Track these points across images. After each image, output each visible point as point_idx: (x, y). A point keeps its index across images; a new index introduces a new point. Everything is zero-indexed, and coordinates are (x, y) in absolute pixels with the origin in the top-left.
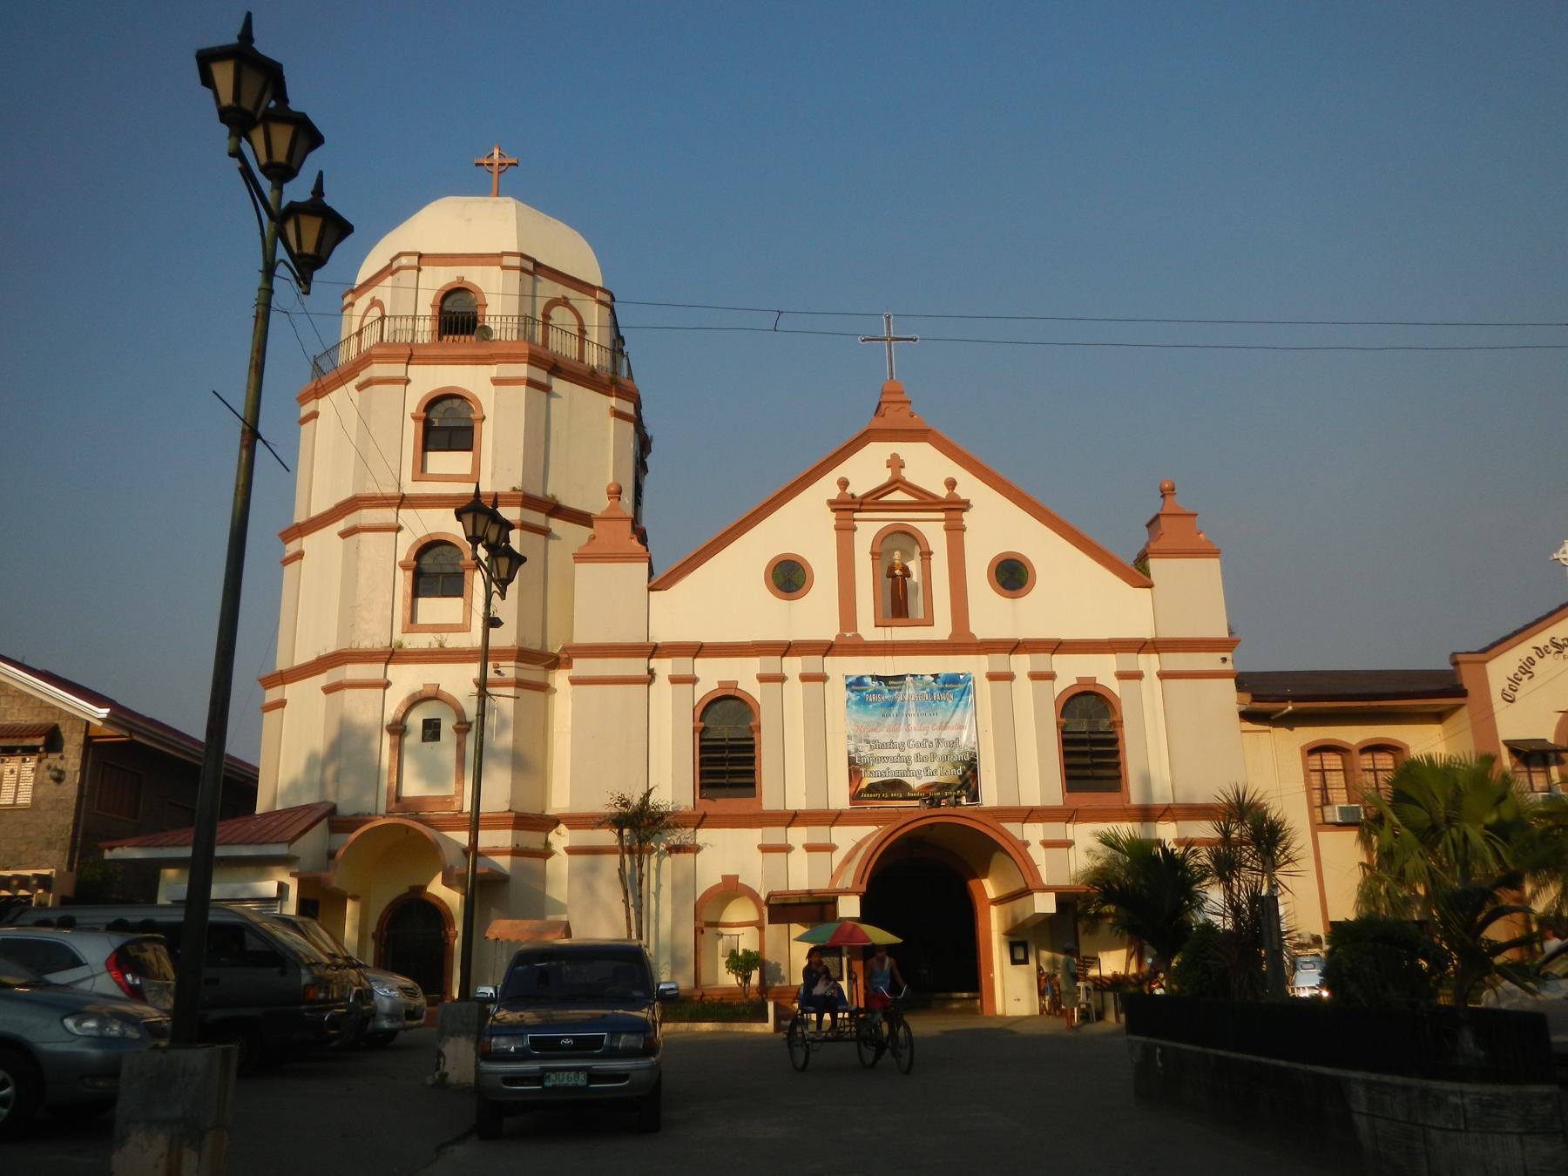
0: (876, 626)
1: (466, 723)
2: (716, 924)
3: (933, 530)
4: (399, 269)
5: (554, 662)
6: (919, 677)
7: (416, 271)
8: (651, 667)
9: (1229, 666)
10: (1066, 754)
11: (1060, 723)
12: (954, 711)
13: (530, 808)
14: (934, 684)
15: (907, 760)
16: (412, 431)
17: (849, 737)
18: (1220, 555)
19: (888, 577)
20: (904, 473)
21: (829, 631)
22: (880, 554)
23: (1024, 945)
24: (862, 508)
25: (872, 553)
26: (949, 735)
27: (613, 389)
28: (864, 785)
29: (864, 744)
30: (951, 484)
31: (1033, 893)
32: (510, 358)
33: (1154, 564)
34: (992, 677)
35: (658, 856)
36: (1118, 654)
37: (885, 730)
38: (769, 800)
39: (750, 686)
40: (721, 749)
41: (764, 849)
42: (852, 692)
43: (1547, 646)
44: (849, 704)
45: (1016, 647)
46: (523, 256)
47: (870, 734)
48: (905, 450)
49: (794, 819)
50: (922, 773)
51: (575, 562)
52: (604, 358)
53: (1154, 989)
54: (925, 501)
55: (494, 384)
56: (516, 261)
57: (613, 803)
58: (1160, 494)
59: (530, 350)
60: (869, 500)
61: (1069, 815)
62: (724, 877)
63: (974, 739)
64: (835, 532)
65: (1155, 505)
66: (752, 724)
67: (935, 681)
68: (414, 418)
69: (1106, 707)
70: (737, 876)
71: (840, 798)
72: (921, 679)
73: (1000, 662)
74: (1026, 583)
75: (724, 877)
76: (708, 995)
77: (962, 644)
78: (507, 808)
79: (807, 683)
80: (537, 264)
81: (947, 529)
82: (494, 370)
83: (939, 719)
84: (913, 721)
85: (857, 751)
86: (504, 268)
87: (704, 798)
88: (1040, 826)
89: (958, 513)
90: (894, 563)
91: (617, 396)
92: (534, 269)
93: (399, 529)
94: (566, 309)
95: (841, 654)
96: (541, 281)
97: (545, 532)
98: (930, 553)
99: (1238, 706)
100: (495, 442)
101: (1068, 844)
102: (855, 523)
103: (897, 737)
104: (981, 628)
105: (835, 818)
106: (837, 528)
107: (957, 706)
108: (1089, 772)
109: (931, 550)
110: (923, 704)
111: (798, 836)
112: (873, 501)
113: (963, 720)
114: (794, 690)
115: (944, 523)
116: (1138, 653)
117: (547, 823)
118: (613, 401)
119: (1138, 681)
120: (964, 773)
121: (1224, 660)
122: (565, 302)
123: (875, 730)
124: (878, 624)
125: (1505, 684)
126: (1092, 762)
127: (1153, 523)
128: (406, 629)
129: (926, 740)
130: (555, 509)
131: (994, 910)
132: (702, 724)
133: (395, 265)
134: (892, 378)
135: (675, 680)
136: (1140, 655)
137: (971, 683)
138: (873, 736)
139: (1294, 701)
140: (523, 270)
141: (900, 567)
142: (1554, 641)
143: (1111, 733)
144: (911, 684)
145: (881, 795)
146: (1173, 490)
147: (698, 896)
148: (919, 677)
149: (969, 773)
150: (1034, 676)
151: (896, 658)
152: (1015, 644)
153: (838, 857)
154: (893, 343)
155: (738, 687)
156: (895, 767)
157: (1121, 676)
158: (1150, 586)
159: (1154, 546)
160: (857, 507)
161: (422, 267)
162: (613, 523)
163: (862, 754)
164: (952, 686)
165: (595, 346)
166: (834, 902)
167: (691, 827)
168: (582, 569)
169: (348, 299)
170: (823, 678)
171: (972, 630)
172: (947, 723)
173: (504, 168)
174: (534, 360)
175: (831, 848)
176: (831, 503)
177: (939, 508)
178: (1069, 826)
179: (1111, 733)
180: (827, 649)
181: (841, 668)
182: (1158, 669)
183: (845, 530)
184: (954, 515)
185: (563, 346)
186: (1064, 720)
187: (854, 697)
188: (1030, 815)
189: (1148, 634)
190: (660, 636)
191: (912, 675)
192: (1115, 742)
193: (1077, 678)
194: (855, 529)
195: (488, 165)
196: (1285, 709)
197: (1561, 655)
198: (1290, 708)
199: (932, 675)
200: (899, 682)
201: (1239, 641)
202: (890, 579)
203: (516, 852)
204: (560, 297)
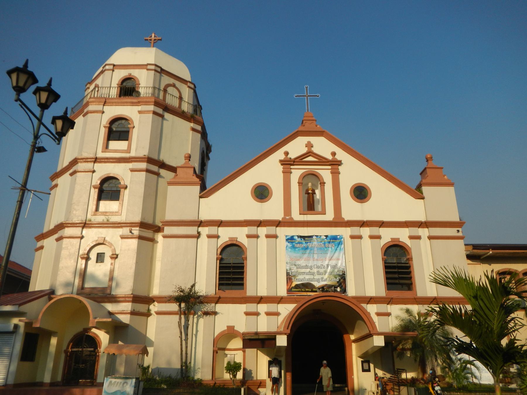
0: (300, 214)
1: (115, 254)
2: (224, 349)
3: (326, 174)
4: (105, 70)
5: (158, 230)
6: (319, 237)
7: (112, 71)
8: (199, 231)
9: (460, 234)
10: (387, 273)
11: (384, 258)
12: (335, 252)
13: (141, 293)
14: (326, 240)
15: (313, 274)
16: (103, 132)
17: (287, 263)
18: (454, 185)
19: (306, 194)
20: (313, 149)
21: (279, 216)
22: (302, 183)
23: (368, 362)
24: (294, 163)
25: (299, 183)
26: (333, 263)
27: (192, 119)
28: (293, 285)
29: (294, 266)
30: (334, 154)
31: (373, 336)
32: (146, 103)
33: (424, 189)
34: (352, 237)
35: (197, 317)
36: (409, 228)
37: (303, 260)
38: (250, 291)
39: (243, 240)
40: (229, 268)
41: (247, 314)
42: (289, 242)
44: (287, 248)
45: (363, 224)
46: (156, 65)
47: (296, 262)
48: (313, 140)
49: (260, 300)
50: (320, 280)
51: (168, 185)
52: (189, 108)
53: (435, 387)
54: (322, 161)
55: (139, 113)
56: (153, 67)
57: (176, 290)
58: (426, 160)
59: (155, 99)
60: (297, 160)
61: (389, 301)
62: (228, 327)
63: (344, 265)
64: (282, 174)
65: (425, 165)
66: (243, 256)
67: (326, 238)
68: (105, 127)
69: (404, 252)
70: (234, 326)
71: (282, 291)
72: (320, 237)
73: (356, 230)
74: (367, 196)
75: (228, 327)
76: (218, 383)
77: (338, 222)
78: (131, 293)
79: (268, 239)
80: (162, 69)
81: (332, 173)
82: (139, 108)
83: (329, 255)
84: (316, 256)
85: (290, 269)
86: (148, 70)
87: (220, 290)
88: (375, 305)
89: (338, 166)
90: (308, 188)
91: (194, 123)
92: (161, 71)
93: (94, 172)
95: (284, 226)
96: (164, 76)
97: (158, 174)
98: (324, 183)
99: (465, 252)
100: (138, 137)
101: (389, 314)
102: (291, 170)
103: (309, 263)
104: (347, 215)
105: (280, 300)
106: (283, 172)
107: (336, 250)
108: (397, 281)
109: (325, 181)
110: (321, 249)
111: (263, 308)
112: (300, 160)
113: (339, 256)
114: (263, 242)
115: (330, 170)
116: (419, 228)
117: (149, 300)
118: (192, 125)
119: (419, 240)
120: (340, 280)
121: (458, 231)
122: (174, 86)
123: (299, 260)
124: (301, 213)
126: (399, 276)
127: (423, 173)
128: (93, 214)
129: (322, 265)
130: (163, 165)
131: (354, 345)
132: (221, 256)
133: (104, 70)
134: (308, 111)
135: (209, 236)
136: (419, 229)
137: (342, 240)
138: (298, 263)
139: (492, 249)
140: (155, 71)
141: (311, 189)
143: (407, 263)
144: (315, 240)
145: (301, 290)
146: (432, 158)
147: (216, 335)
148: (319, 237)
149: (342, 280)
150: (371, 237)
151: (308, 228)
152: (363, 223)
153: (281, 318)
154: (309, 97)
155: (238, 240)
156: (307, 277)
157: (411, 237)
158: (423, 198)
159: (424, 181)
160: (292, 163)
161: (114, 70)
162: (185, 169)
163: (293, 271)
164: (334, 241)
165: (187, 103)
166: (275, 339)
167: (213, 303)
168: (171, 188)
169: (88, 86)
170: (275, 237)
171: (343, 216)
172: (332, 257)
173: (156, 41)
174: (157, 104)
175: (277, 314)
176: (281, 161)
177: (328, 164)
178: (389, 306)
179: (407, 263)
180: (278, 224)
181: (284, 232)
182: (428, 235)
183: (287, 173)
184: (335, 167)
185: (172, 101)
186: (385, 257)
187: (289, 245)
188: (371, 300)
189: (423, 219)
190: (204, 216)
191: (317, 236)
192: (409, 267)
193: (391, 238)
194: (291, 173)
195: (150, 40)
196: (489, 253)
198: (491, 252)
199: (325, 236)
200: (310, 239)
201: (465, 223)
202: (307, 195)
203: (133, 313)
204: (172, 83)
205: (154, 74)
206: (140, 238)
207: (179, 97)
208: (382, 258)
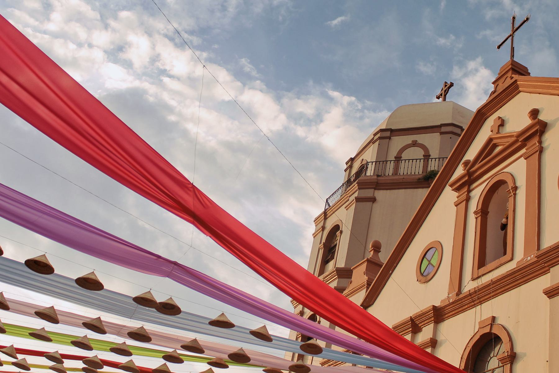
30: (534, 113)
46: (382, 130)
56: (378, 135)
122: (415, 144)
160: (466, 178)
205: (379, 144)
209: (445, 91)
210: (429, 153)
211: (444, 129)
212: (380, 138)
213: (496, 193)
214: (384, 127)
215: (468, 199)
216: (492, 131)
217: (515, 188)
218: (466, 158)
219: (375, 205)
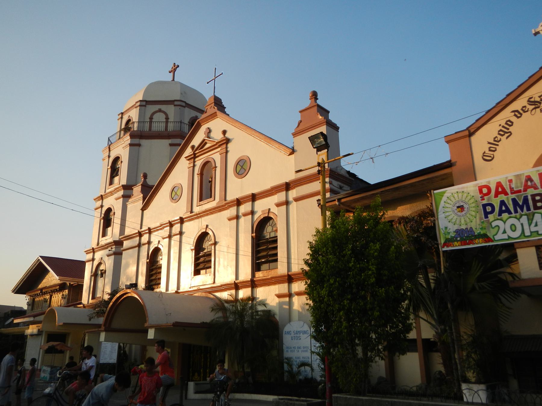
0: (197, 206)
3: (216, 156)
30: (224, 132)
43: (525, 107)
46: (140, 101)
56: (139, 104)
86: (136, 107)
94: (161, 113)
122: (160, 111)
125: (485, 148)
142: (532, 100)
160: (193, 156)
197: (538, 110)
204: (158, 110)
206: (115, 254)
207: (165, 118)
208: (252, 237)
209: (174, 69)
210: (168, 116)
211: (176, 103)
212: (140, 106)
213: (206, 166)
214: (141, 99)
215: (194, 166)
216: (205, 134)
217: (216, 167)
218: (192, 144)
219: (141, 148)
